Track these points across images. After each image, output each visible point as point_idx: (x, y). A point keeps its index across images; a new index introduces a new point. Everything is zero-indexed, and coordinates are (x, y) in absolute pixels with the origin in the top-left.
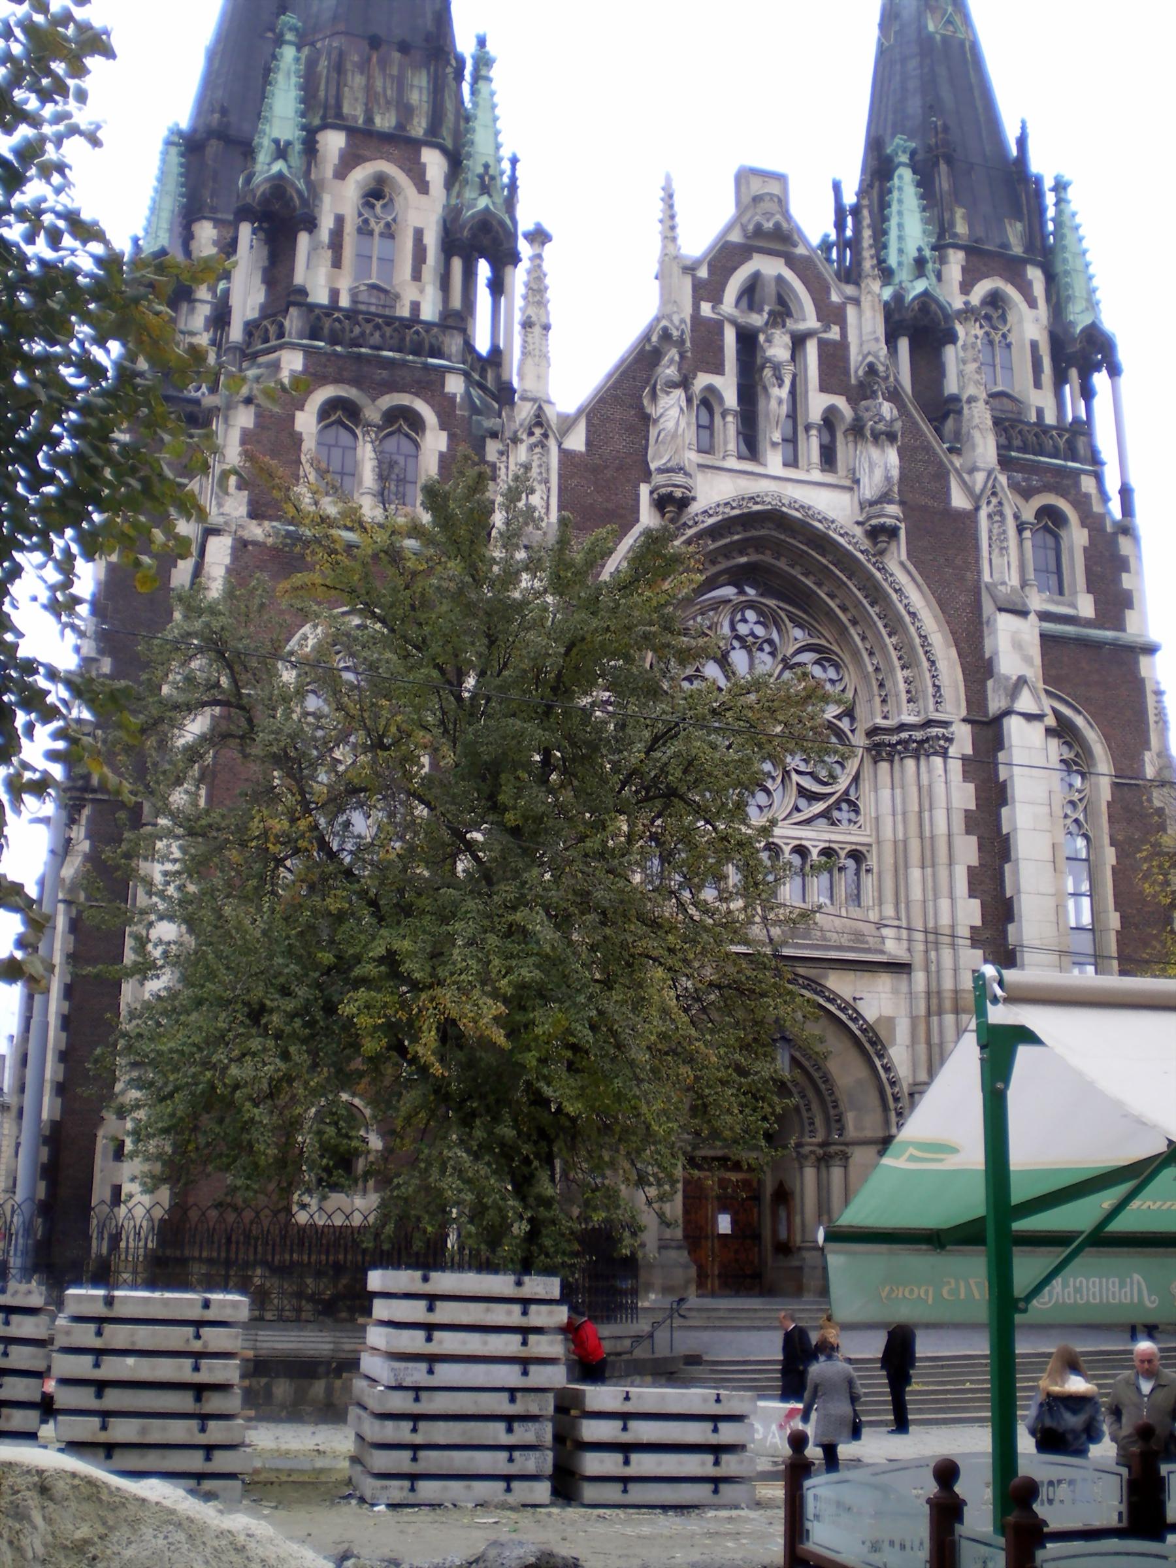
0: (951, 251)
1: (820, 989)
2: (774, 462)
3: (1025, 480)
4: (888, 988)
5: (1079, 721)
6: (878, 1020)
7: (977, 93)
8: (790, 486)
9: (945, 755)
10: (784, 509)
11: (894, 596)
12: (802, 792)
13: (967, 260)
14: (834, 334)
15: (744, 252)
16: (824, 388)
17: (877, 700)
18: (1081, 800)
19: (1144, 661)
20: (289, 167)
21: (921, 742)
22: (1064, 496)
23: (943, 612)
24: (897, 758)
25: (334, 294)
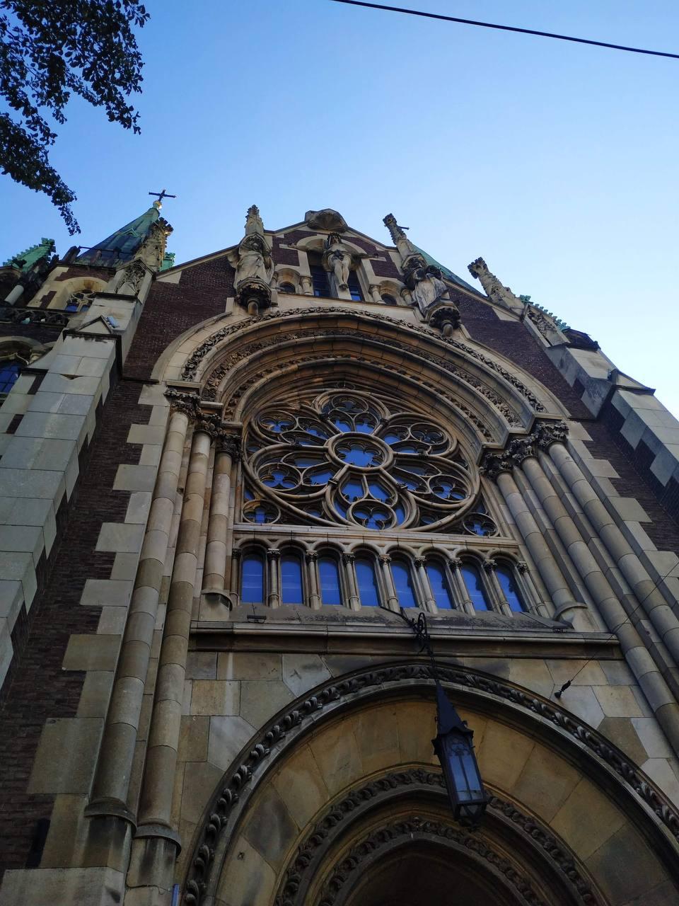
1: (502, 687)
4: (602, 681)
6: (606, 722)
9: (565, 442)
10: (356, 315)
14: (384, 259)
17: (480, 434)
21: (535, 443)
23: (518, 363)
24: (515, 468)
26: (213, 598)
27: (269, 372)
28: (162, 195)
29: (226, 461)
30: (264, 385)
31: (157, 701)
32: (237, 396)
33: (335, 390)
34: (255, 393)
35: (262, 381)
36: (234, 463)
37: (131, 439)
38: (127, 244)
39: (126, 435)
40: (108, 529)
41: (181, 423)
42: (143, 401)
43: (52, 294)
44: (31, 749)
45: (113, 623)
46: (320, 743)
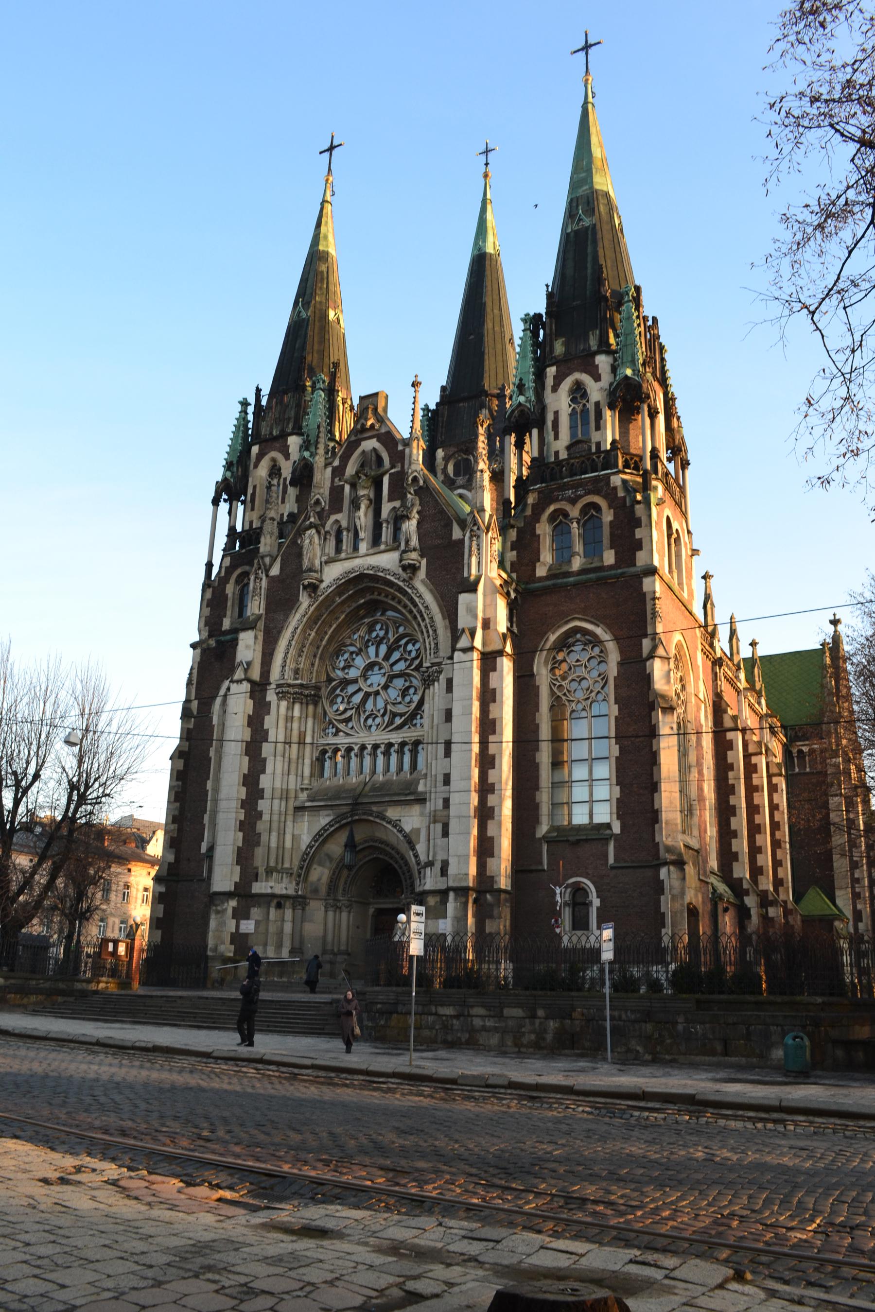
0: (548, 370)
1: (384, 818)
2: (363, 547)
3: (572, 493)
5: (598, 631)
6: (411, 831)
7: (589, 259)
8: (368, 558)
9: (438, 680)
11: (417, 600)
12: (394, 715)
13: (557, 371)
15: (358, 443)
16: (390, 500)
18: (602, 679)
19: (646, 581)
20: (232, 473)
22: (597, 492)
23: (443, 601)
25: (251, 523)
26: (302, 789)
27: (331, 626)
28: (331, 149)
29: (311, 708)
30: (329, 639)
31: (284, 834)
32: (315, 656)
33: (370, 620)
34: (325, 647)
35: (327, 637)
36: (316, 704)
37: (265, 727)
38: (297, 346)
39: (263, 724)
40: (262, 776)
41: (284, 704)
42: (268, 699)
43: (255, 487)
44: (253, 855)
45: (266, 817)
46: (337, 836)
